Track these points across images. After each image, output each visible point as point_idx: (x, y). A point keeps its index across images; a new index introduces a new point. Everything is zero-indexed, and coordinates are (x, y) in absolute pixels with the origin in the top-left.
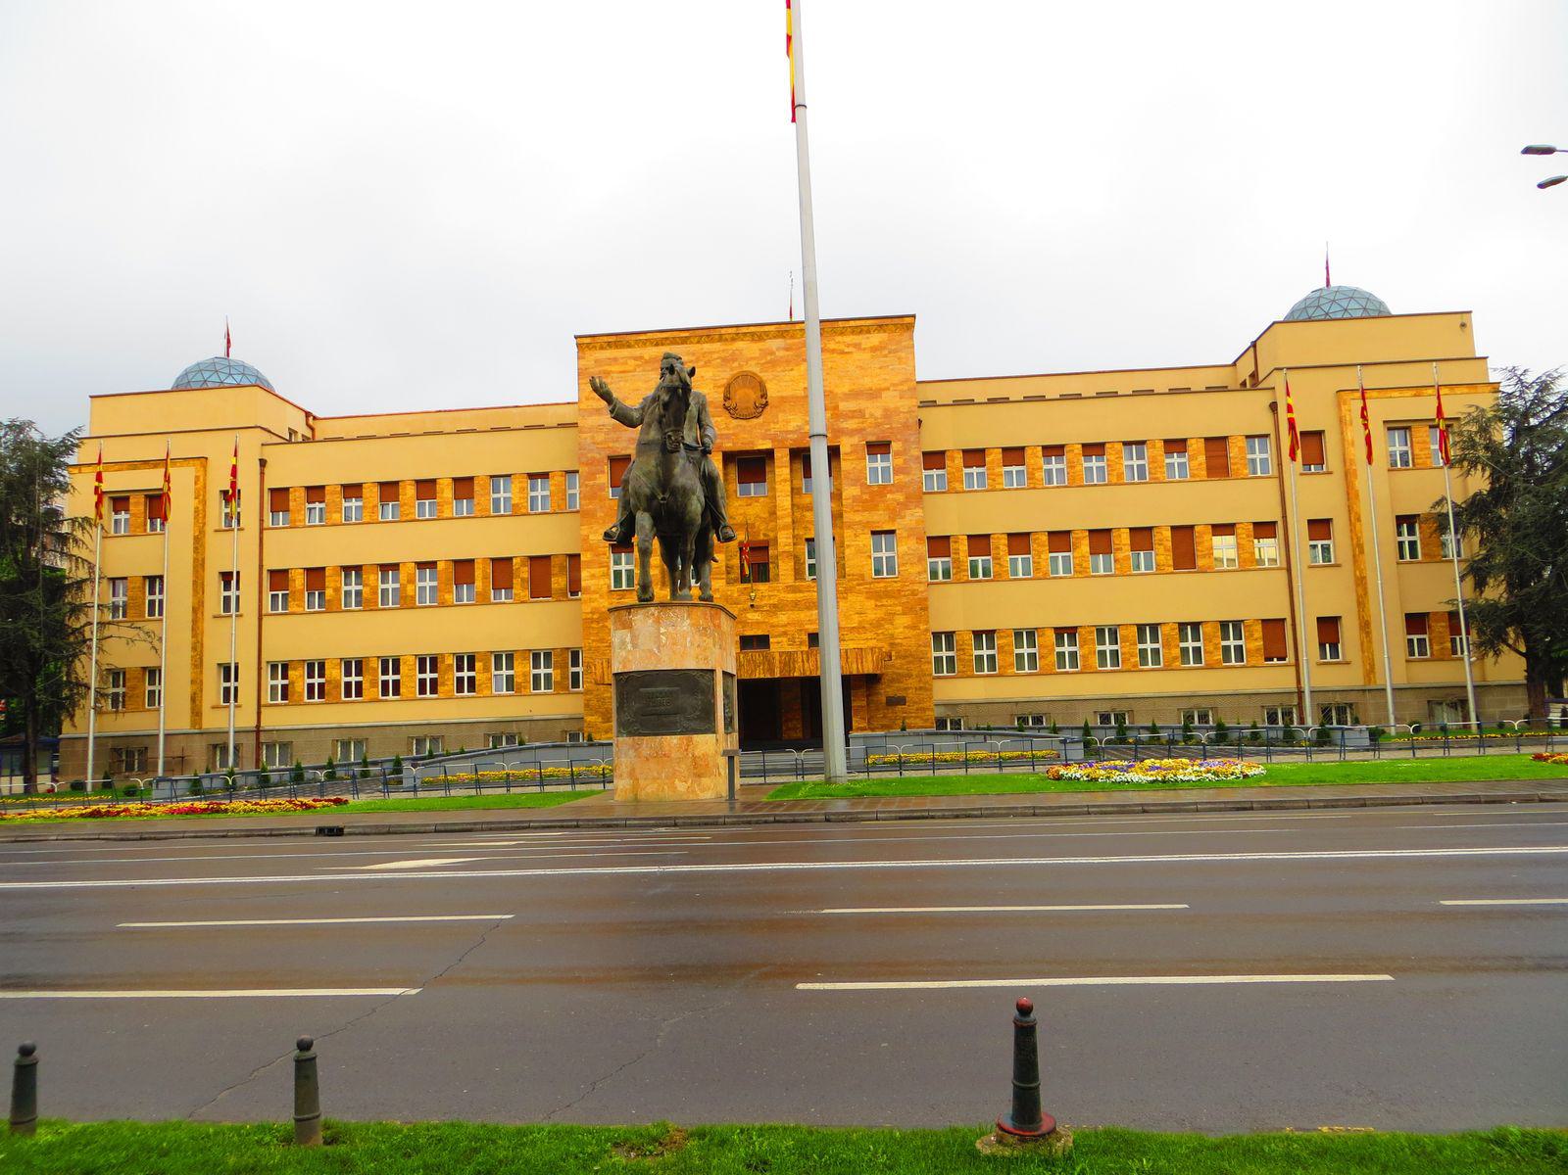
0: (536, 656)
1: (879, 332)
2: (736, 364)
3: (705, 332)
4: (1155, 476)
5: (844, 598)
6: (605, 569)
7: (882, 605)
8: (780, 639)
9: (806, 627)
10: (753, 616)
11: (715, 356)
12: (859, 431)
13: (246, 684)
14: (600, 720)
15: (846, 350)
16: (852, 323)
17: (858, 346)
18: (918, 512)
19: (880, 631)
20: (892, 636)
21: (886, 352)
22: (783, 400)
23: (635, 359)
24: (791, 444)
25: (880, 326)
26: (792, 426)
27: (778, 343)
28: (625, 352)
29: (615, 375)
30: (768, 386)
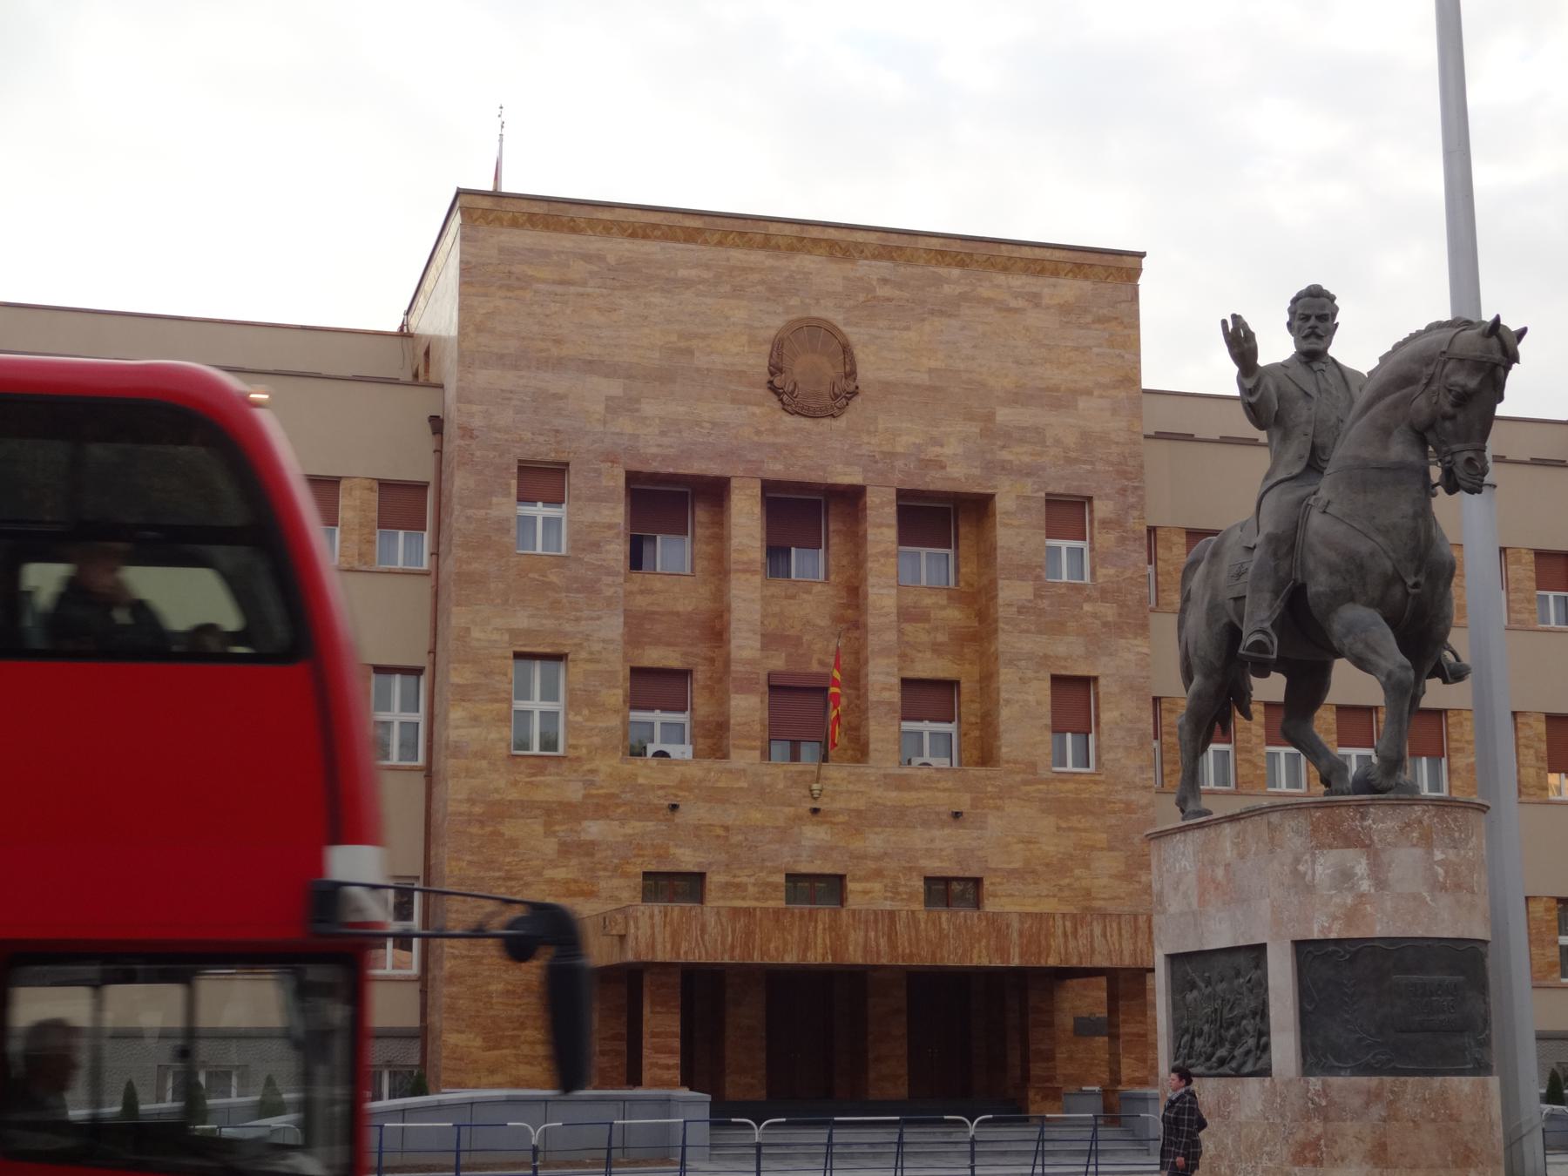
1: (1075, 277)
2: (794, 301)
3: (738, 224)
4: (1519, 617)
5: (998, 808)
6: (505, 706)
7: (1070, 829)
8: (868, 886)
9: (923, 863)
10: (814, 834)
11: (756, 277)
12: (1028, 472)
14: (478, 1042)
15: (1013, 304)
16: (1027, 252)
17: (1035, 299)
18: (1140, 645)
19: (1067, 881)
20: (1088, 894)
21: (1089, 318)
22: (888, 388)
23: (587, 258)
24: (898, 479)
25: (1079, 266)
26: (903, 444)
27: (883, 267)
28: (567, 242)
29: (541, 286)
30: (860, 354)
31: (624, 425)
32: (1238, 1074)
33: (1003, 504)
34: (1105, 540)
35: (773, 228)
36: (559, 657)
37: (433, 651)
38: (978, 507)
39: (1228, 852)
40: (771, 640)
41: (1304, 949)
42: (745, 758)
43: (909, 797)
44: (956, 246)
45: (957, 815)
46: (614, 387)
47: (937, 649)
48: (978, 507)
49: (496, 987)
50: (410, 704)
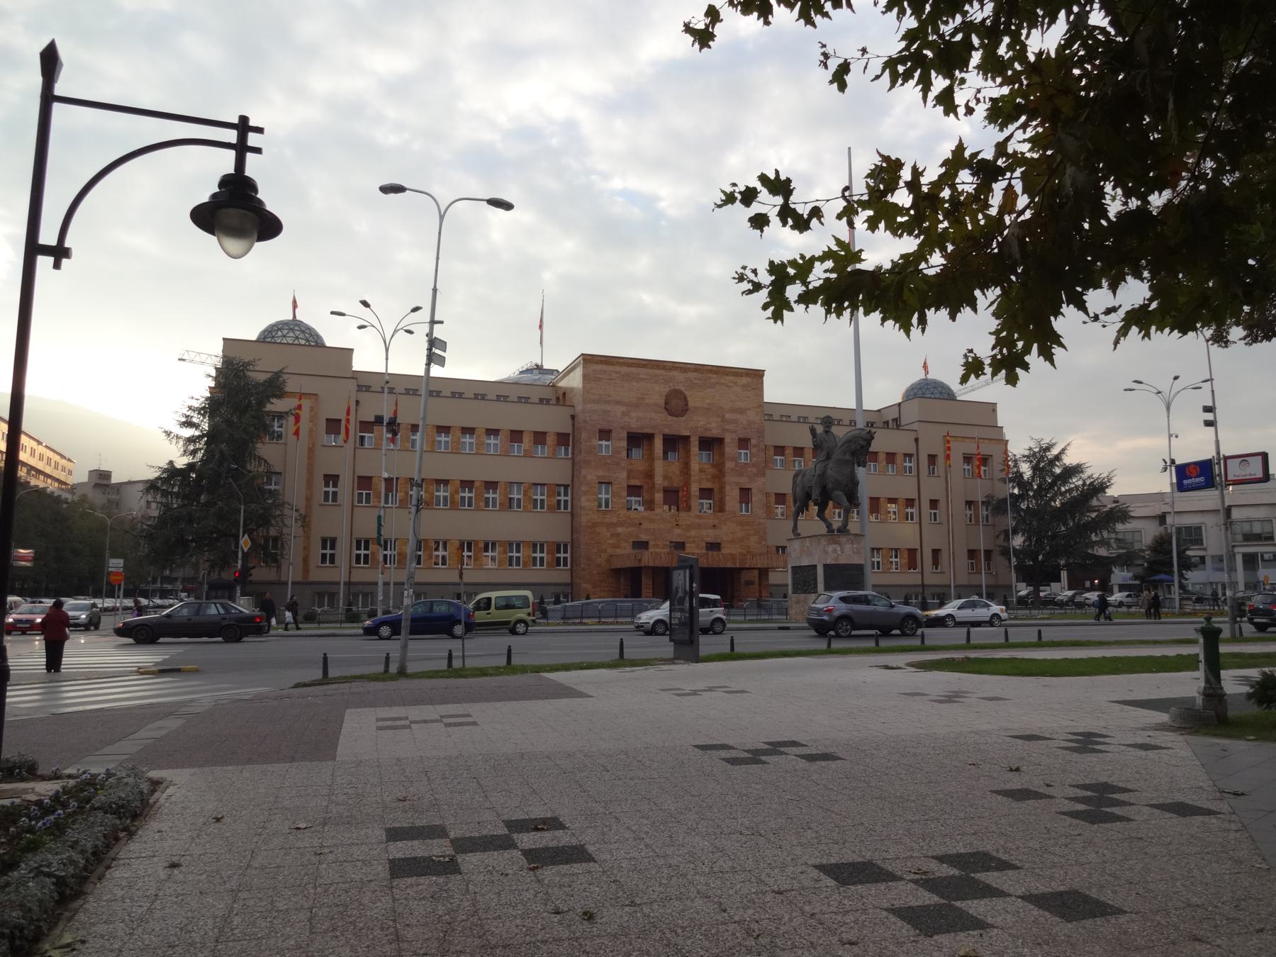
0: (535, 545)
2: (671, 384)
10: (677, 531)
12: (734, 432)
13: (343, 551)
17: (736, 383)
18: (763, 479)
22: (696, 408)
23: (616, 372)
26: (701, 423)
28: (610, 368)
30: (689, 399)
31: (626, 419)
32: (810, 593)
33: (727, 440)
34: (754, 450)
35: (666, 364)
36: (609, 483)
37: (573, 481)
38: (720, 441)
39: (808, 544)
40: (665, 477)
41: (826, 566)
42: (658, 511)
43: (702, 521)
44: (715, 369)
45: (714, 526)
46: (624, 409)
47: (708, 480)
48: (720, 441)
49: (595, 572)
50: (566, 495)
